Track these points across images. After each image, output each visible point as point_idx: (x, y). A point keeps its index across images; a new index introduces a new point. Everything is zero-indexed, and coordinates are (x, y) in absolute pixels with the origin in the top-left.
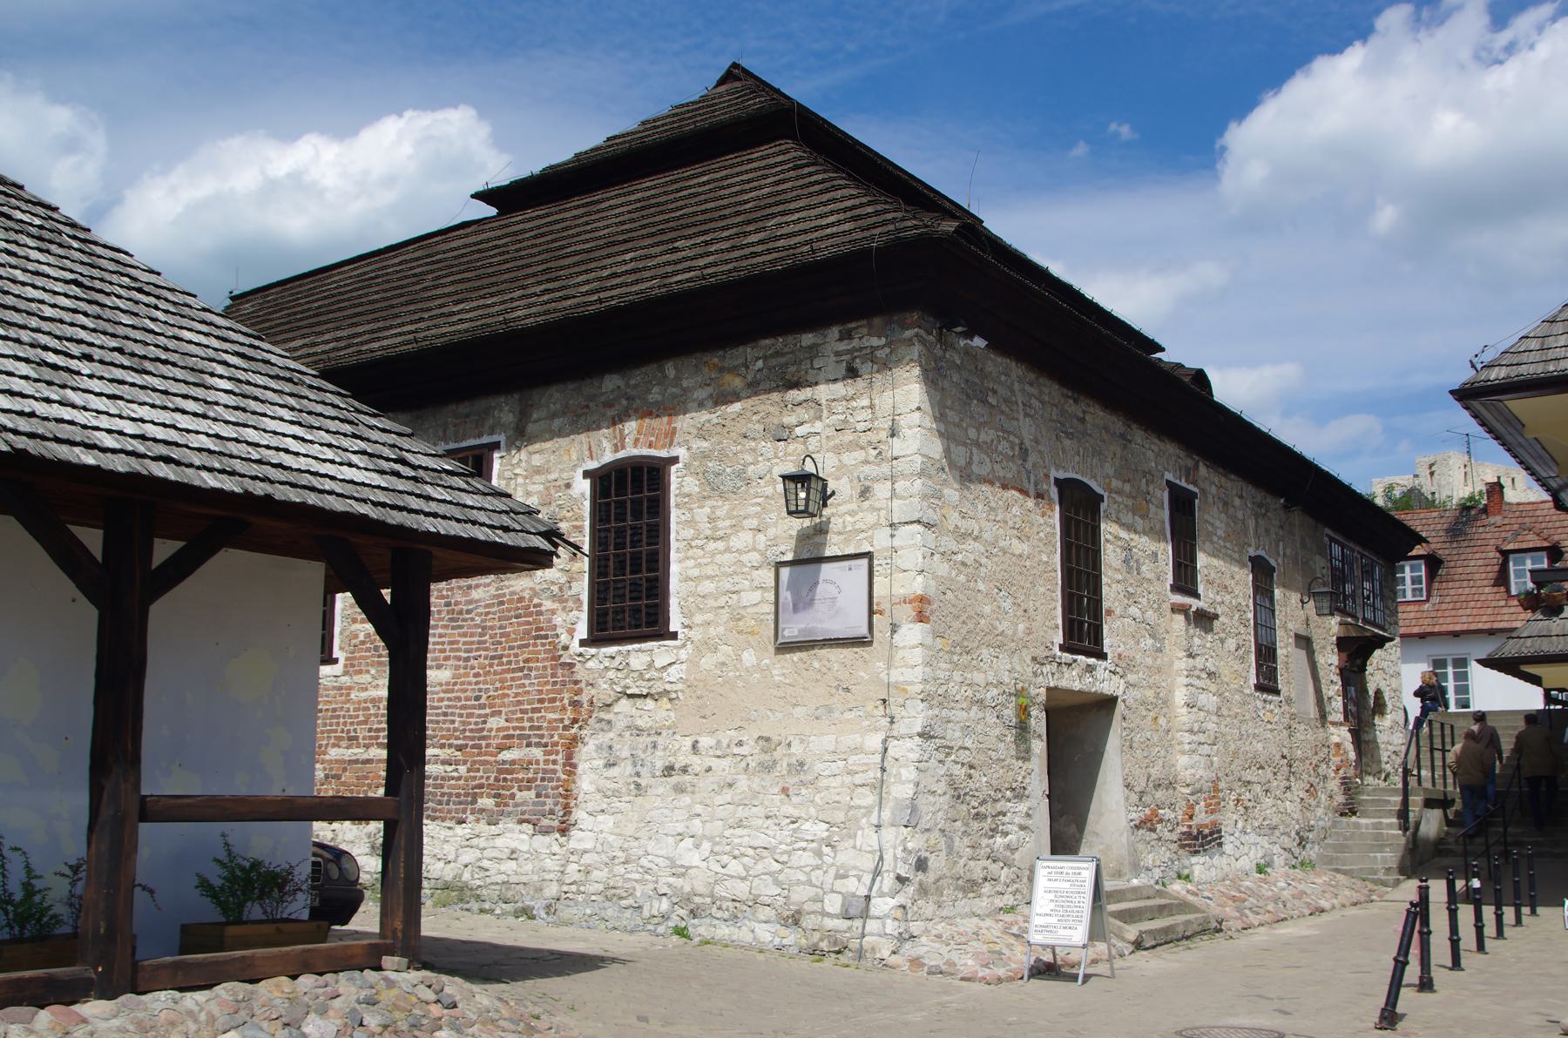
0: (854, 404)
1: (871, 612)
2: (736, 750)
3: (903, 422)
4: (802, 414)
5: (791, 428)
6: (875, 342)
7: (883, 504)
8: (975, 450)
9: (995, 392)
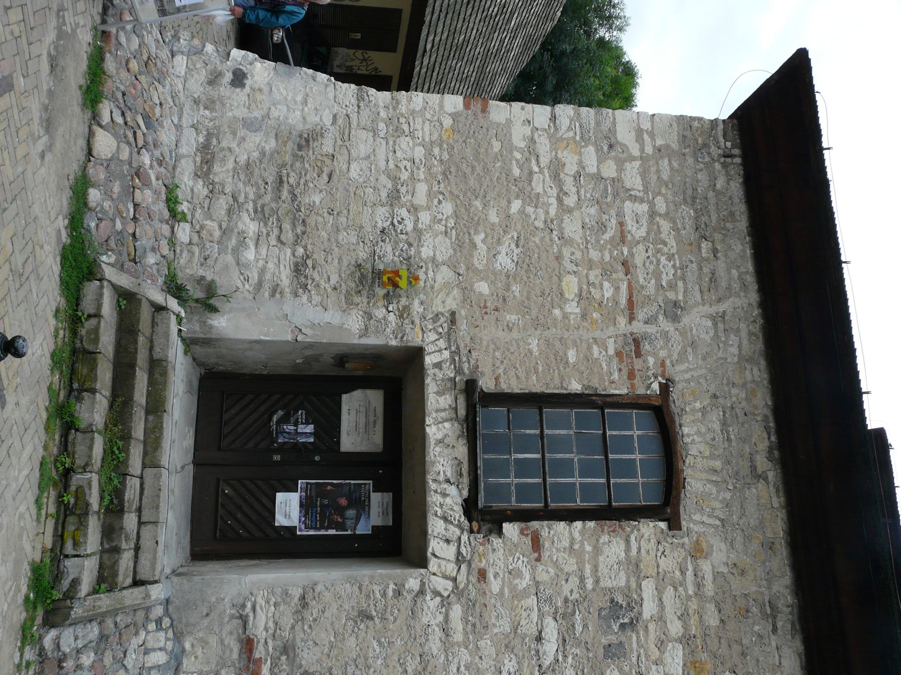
8: (645, 207)
9: (715, 251)
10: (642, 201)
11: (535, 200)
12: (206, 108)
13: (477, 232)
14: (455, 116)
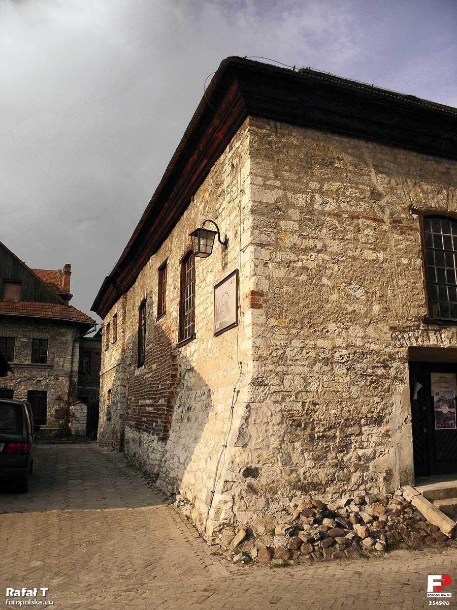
1: (237, 308)
8: (317, 196)
10: (313, 197)
11: (321, 268)
12: (276, 493)
13: (345, 309)
14: (268, 316)
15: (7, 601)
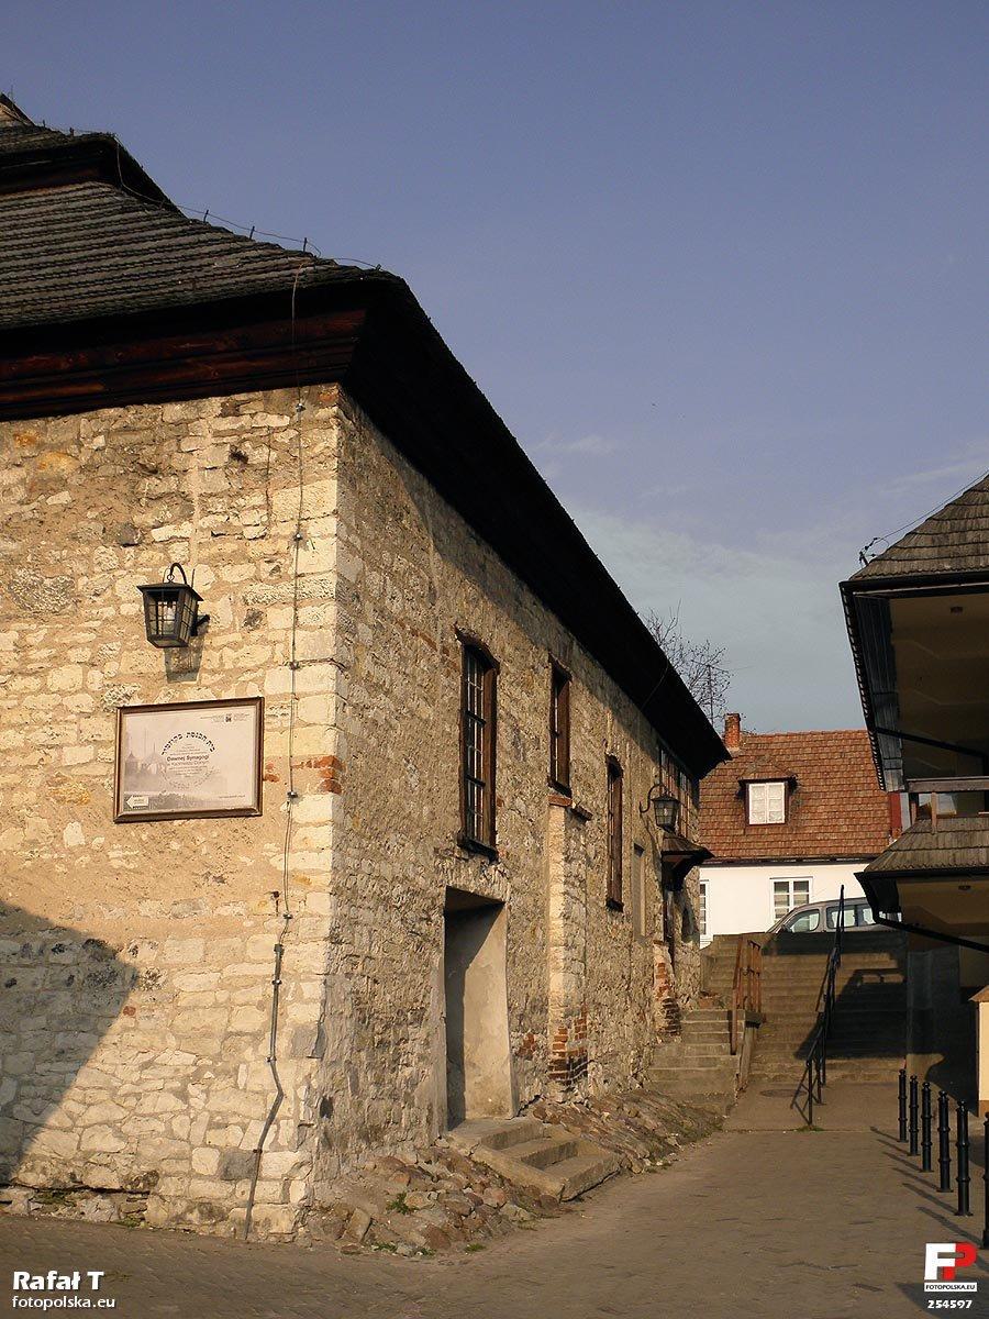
0: (241, 502)
1: (260, 779)
2: (54, 958)
3: (312, 529)
4: (163, 511)
5: (146, 530)
6: (274, 421)
7: (280, 636)
15: (14, 1300)
